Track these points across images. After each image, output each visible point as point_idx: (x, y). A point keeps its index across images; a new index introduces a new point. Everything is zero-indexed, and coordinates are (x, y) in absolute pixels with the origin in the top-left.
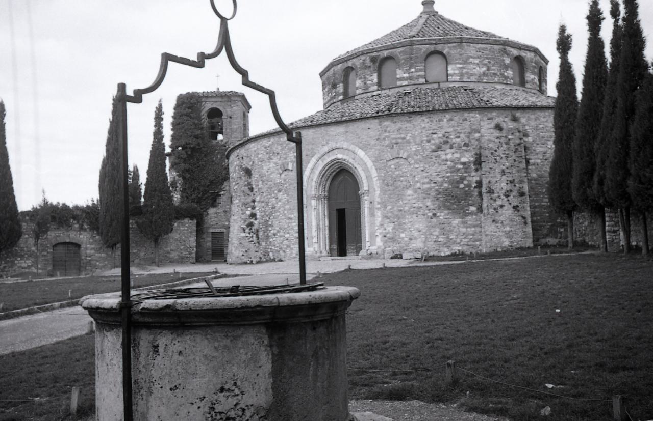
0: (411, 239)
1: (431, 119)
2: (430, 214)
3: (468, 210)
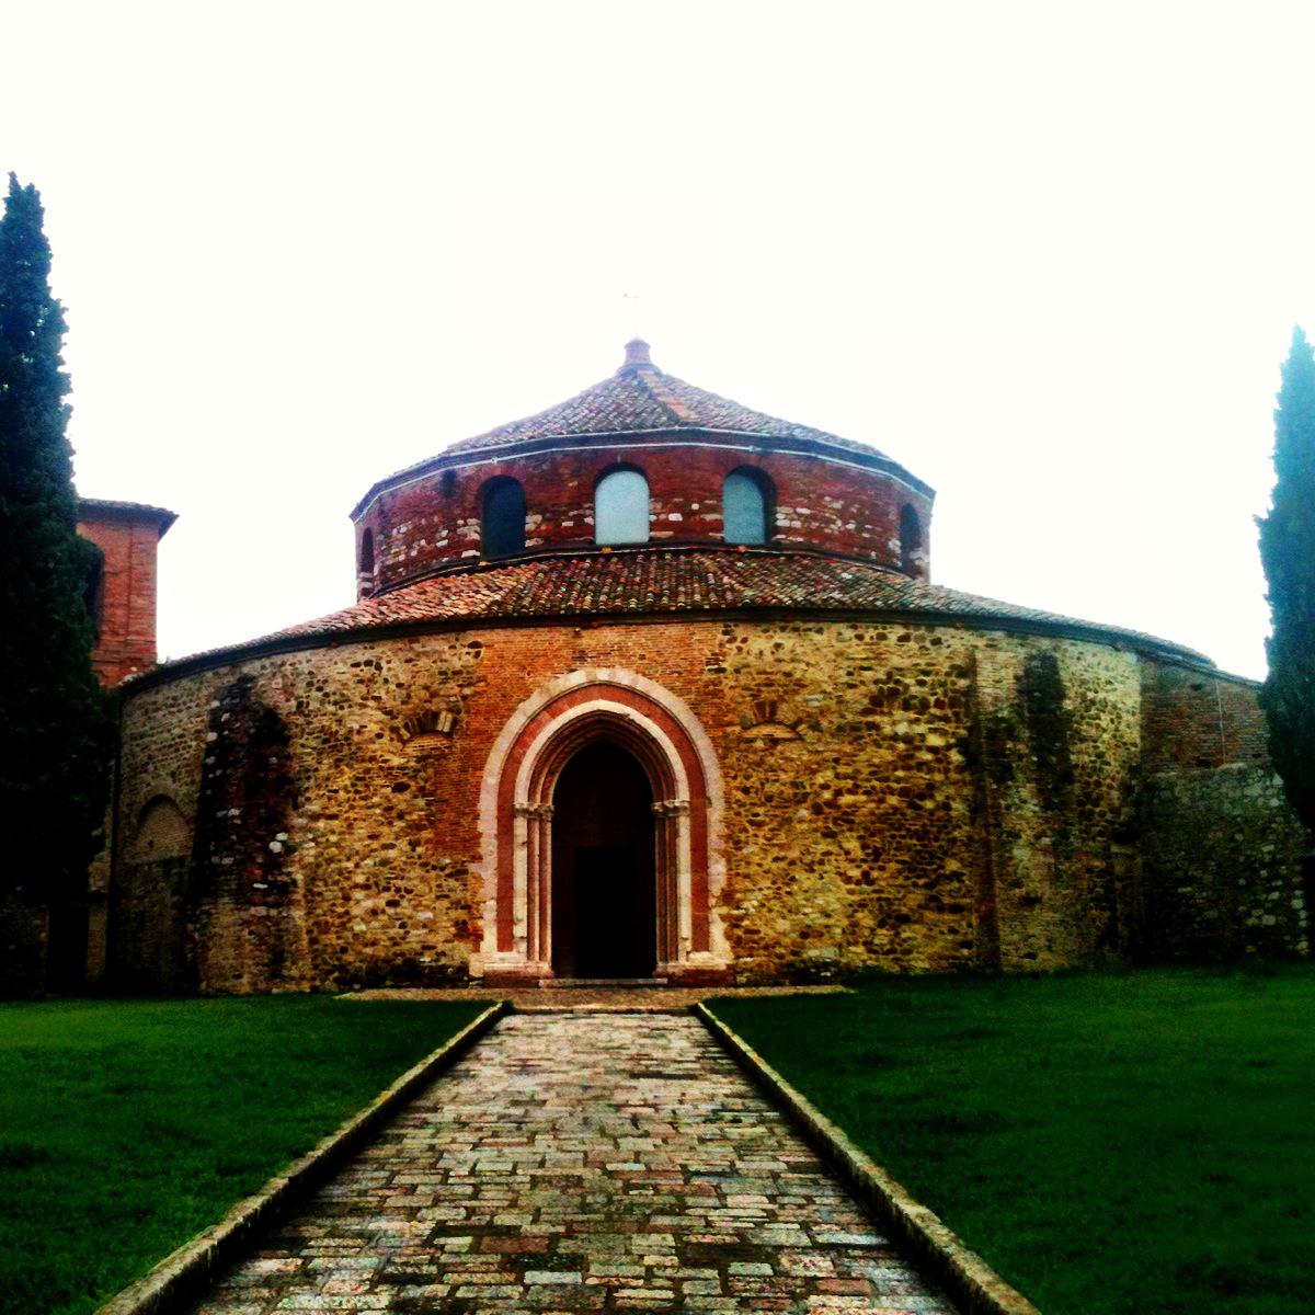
0: (804, 935)
1: (860, 632)
2: (855, 873)
3: (943, 867)
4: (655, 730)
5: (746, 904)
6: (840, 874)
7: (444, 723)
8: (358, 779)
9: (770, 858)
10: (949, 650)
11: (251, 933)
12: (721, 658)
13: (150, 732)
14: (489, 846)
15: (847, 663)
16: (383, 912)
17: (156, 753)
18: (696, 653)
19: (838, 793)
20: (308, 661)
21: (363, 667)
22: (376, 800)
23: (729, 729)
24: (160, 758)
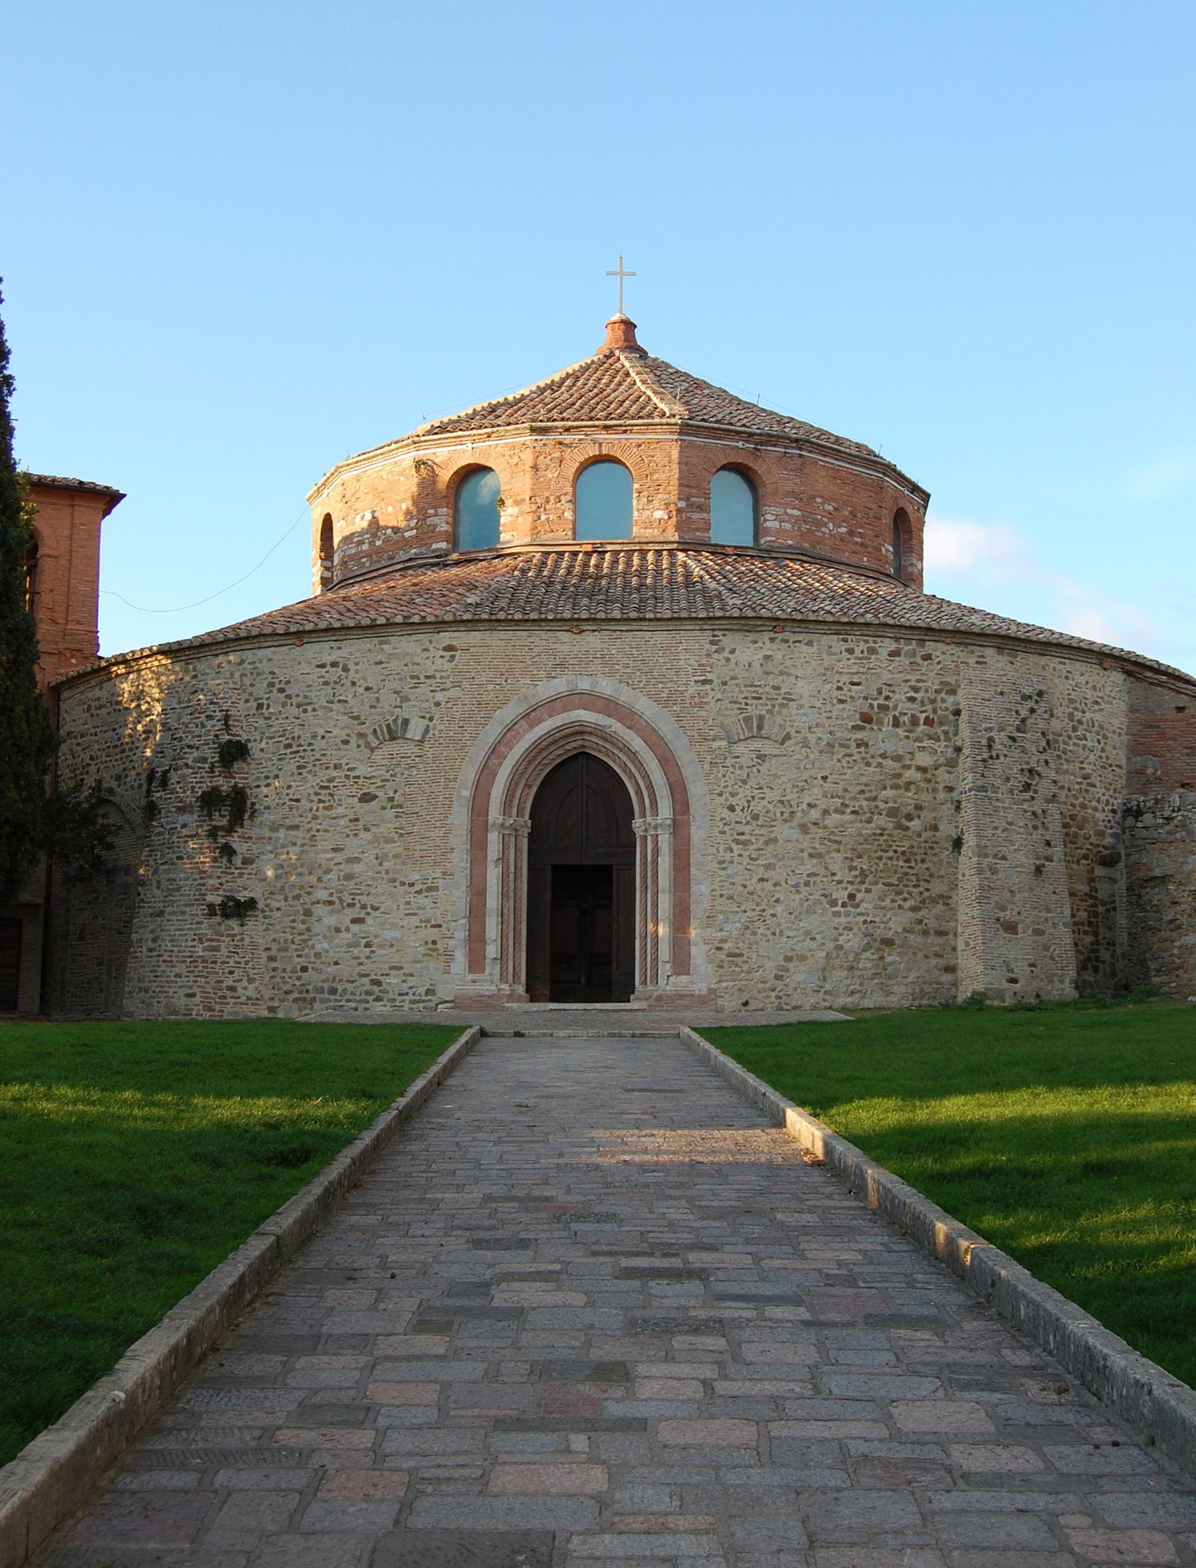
2: (841, 895)
4: (637, 744)
5: (727, 927)
6: (826, 896)
7: (414, 731)
8: (322, 787)
9: (755, 880)
10: (939, 667)
11: (205, 949)
12: (708, 669)
13: (93, 731)
14: (460, 859)
15: (837, 677)
16: (348, 930)
17: (99, 753)
18: (681, 662)
19: (826, 812)
20: (270, 660)
21: (328, 668)
22: (340, 810)
23: (715, 745)
24: (104, 759)
